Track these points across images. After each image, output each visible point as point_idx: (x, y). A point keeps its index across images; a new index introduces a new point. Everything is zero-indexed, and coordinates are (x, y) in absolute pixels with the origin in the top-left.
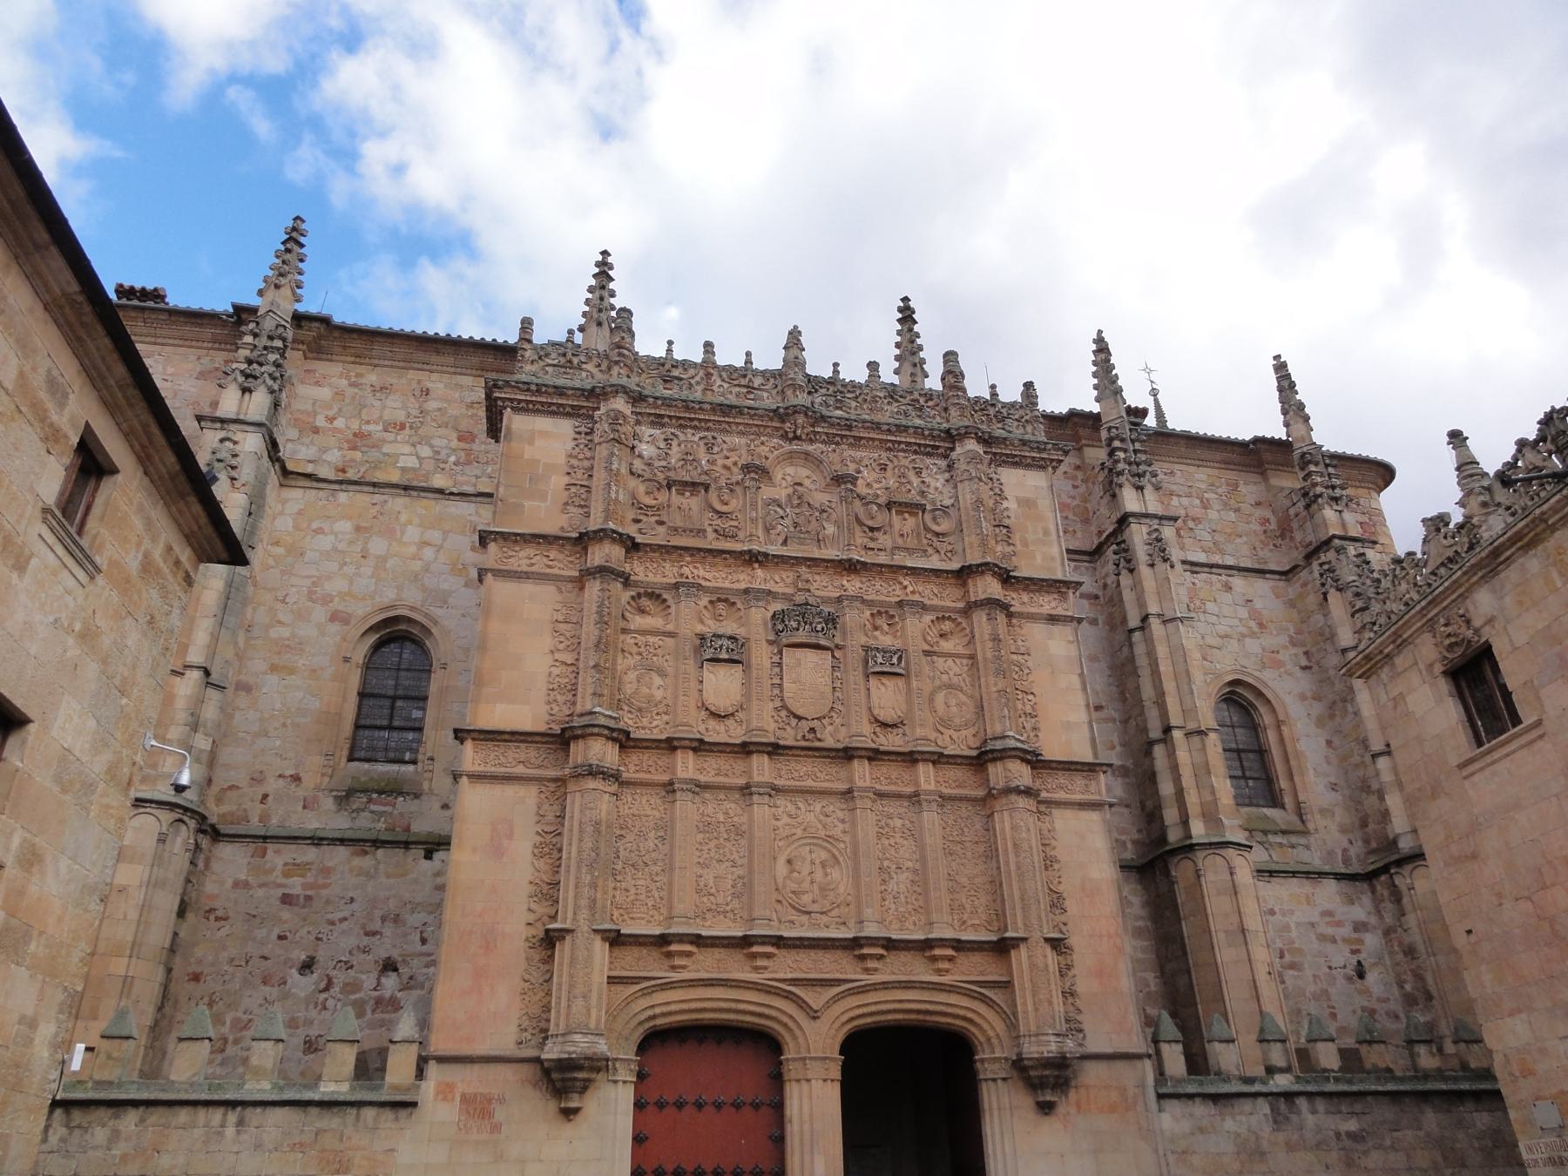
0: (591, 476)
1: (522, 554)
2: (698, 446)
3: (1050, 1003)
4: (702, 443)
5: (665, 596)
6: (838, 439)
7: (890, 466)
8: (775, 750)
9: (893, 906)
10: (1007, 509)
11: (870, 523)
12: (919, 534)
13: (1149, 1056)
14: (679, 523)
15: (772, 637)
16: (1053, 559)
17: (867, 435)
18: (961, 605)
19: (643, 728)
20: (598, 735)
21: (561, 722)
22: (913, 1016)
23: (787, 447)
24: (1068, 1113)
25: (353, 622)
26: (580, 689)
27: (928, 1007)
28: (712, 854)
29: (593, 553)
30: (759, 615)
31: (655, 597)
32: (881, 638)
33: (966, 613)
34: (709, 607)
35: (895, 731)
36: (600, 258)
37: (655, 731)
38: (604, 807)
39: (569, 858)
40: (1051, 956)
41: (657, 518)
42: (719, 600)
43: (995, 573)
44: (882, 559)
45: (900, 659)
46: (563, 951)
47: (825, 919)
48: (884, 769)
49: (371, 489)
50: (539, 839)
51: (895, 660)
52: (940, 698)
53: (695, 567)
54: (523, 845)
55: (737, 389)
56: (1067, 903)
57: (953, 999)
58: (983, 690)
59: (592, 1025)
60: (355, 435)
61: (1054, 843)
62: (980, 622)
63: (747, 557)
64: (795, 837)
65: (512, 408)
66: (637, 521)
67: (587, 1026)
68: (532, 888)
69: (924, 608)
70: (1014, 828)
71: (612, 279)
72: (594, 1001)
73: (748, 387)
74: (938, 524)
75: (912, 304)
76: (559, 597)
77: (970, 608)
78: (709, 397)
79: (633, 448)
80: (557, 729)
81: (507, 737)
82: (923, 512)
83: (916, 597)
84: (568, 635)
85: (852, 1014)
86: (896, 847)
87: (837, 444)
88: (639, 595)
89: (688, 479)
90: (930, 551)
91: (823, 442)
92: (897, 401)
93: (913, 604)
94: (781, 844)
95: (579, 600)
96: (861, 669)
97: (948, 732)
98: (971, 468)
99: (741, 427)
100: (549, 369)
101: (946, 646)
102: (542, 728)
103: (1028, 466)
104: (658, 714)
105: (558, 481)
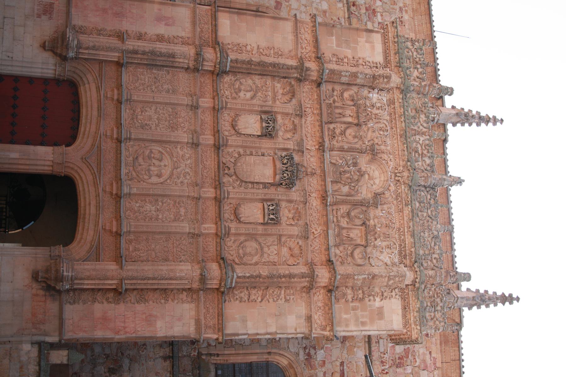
1: (307, 36)
3: (88, 278)
5: (294, 100)
8: (217, 147)
9: (138, 205)
10: (375, 300)
11: (353, 214)
13: (60, 341)
16: (347, 325)
22: (82, 212)
24: (32, 288)
25: (276, 11)
27: (87, 220)
28: (161, 115)
30: (290, 145)
38: (181, 60)
39: (157, 44)
40: (112, 283)
41: (336, 99)
45: (272, 219)
46: (114, 42)
47: (131, 168)
49: (347, 16)
50: (166, 36)
51: (272, 216)
52: (254, 245)
54: (162, 30)
55: (420, 148)
56: (143, 305)
57: (91, 233)
59: (81, 51)
60: (374, 10)
61: (176, 301)
64: (172, 156)
65: (384, 33)
67: (81, 48)
68: (143, 32)
70: (182, 270)
72: (91, 52)
73: (422, 153)
74: (358, 254)
81: (214, 23)
83: (311, 237)
85: (84, 178)
86: (169, 210)
87: (397, 199)
94: (168, 149)
99: (396, 145)
100: (411, 53)
101: (285, 250)
102: (220, 39)
103: (404, 316)
105: (349, 53)
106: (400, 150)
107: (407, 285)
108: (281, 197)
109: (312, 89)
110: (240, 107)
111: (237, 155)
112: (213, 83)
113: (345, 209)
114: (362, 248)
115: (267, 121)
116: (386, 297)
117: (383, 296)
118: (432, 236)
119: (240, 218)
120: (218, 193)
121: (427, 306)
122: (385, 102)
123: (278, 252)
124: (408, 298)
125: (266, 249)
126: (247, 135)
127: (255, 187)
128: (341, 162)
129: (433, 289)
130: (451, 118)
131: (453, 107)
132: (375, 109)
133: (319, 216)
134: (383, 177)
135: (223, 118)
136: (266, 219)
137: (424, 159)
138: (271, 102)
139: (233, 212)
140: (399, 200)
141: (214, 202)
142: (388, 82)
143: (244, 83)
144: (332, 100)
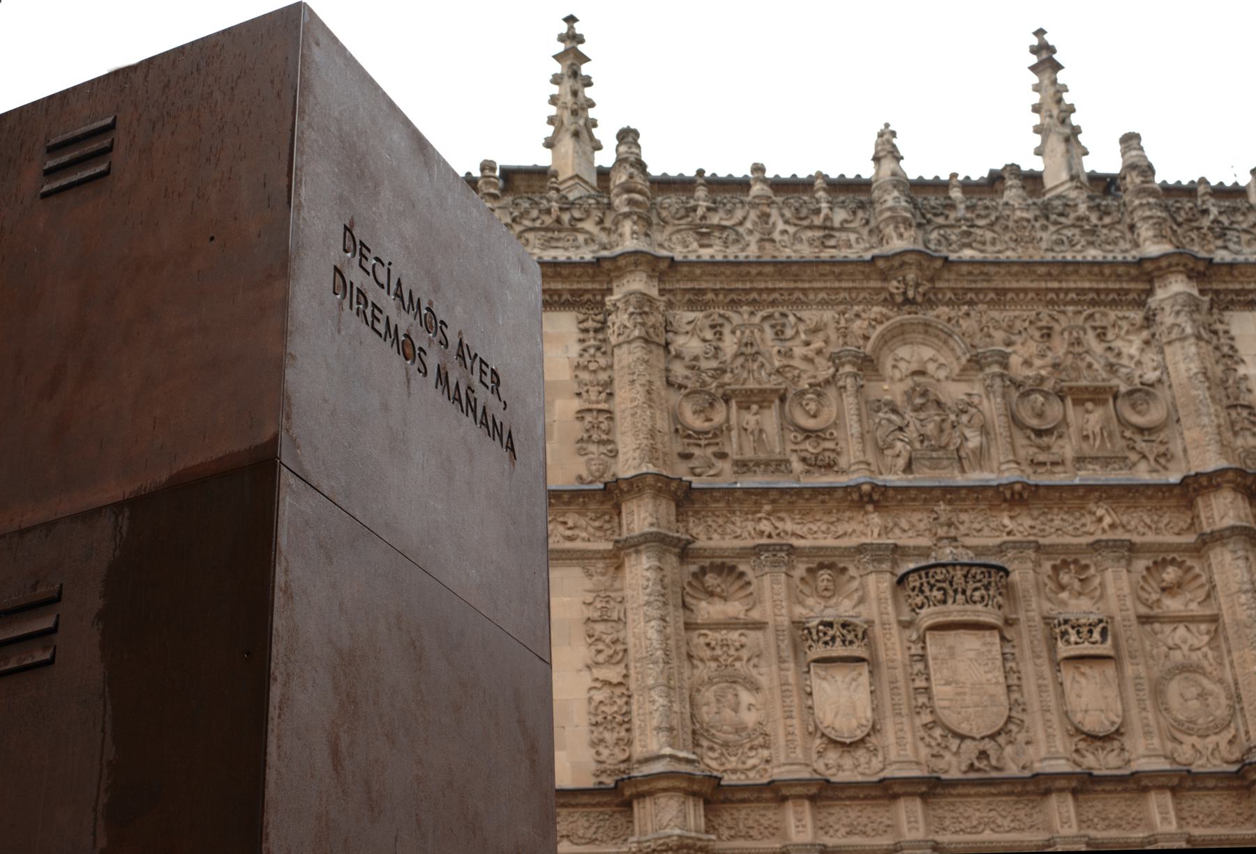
0: (611, 395)
2: (762, 330)
4: (767, 327)
6: (970, 295)
7: (1057, 328)
10: (1245, 378)
11: (1034, 423)
12: (1111, 435)
14: (749, 454)
15: (906, 617)
17: (1015, 285)
18: (1190, 538)
19: (734, 771)
20: (674, 789)
21: (613, 773)
23: (898, 318)
26: (636, 722)
29: (632, 513)
30: (879, 584)
31: (726, 569)
32: (1073, 602)
33: (1198, 550)
34: (808, 578)
35: (1108, 746)
36: (564, 28)
37: (751, 774)
42: (822, 566)
43: (1238, 485)
44: (1060, 478)
45: (1104, 633)
48: (1099, 806)
51: (1096, 636)
52: (1174, 688)
53: (781, 519)
55: (810, 234)
58: (1238, 670)
62: (1221, 563)
63: (855, 496)
66: (687, 457)
69: (1132, 549)
71: (586, 59)
73: (825, 228)
74: (1140, 413)
75: (1050, 39)
76: (589, 584)
77: (1208, 541)
78: (769, 253)
79: (667, 344)
80: (609, 782)
82: (1115, 397)
83: (1120, 535)
84: (608, 639)
87: (971, 303)
88: (703, 571)
89: (751, 385)
90: (1133, 457)
91: (949, 303)
92: (1056, 223)
93: (1115, 545)
95: (617, 585)
96: (1045, 654)
97: (1189, 740)
98: (1183, 319)
99: (822, 295)
101: (1173, 605)
102: (589, 782)
104: (751, 748)
106: (837, 285)
107: (1202, 292)
108: (1033, 610)
109: (697, 512)
110: (795, 722)
111: (938, 732)
112: (731, 801)
113: (1025, 442)
114: (1119, 402)
115: (826, 643)
116: (1232, 347)
117: (1231, 357)
118: (1043, 221)
119: (1113, 723)
120: (1061, 783)
121: (1226, 248)
122: (700, 315)
123: (1180, 622)
124: (1227, 291)
125: (1177, 656)
126: (872, 701)
127: (1016, 682)
128: (899, 445)
129: (1180, 231)
130: (585, 153)
131: (549, 144)
132: (720, 344)
133: (1060, 509)
134: (915, 335)
135: (833, 771)
136: (1106, 649)
137: (837, 224)
138: (759, 634)
139: (1099, 744)
140: (973, 296)
141: (1081, 797)
142: (650, 300)
143: (715, 710)
144: (719, 464)
